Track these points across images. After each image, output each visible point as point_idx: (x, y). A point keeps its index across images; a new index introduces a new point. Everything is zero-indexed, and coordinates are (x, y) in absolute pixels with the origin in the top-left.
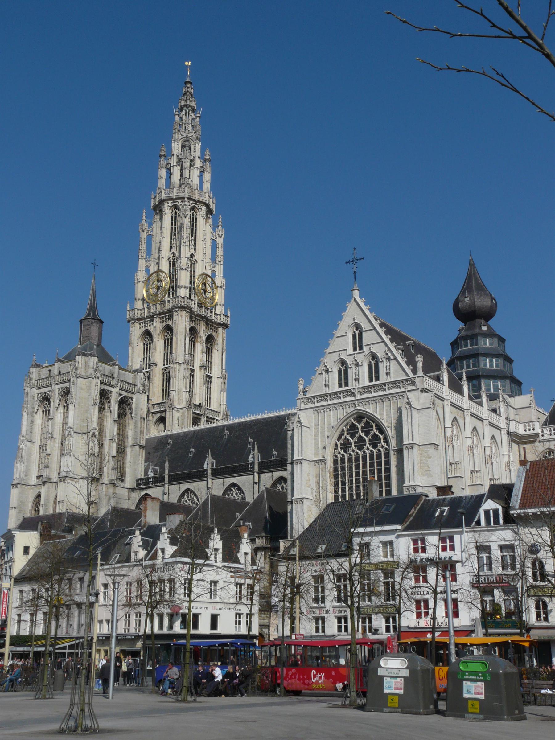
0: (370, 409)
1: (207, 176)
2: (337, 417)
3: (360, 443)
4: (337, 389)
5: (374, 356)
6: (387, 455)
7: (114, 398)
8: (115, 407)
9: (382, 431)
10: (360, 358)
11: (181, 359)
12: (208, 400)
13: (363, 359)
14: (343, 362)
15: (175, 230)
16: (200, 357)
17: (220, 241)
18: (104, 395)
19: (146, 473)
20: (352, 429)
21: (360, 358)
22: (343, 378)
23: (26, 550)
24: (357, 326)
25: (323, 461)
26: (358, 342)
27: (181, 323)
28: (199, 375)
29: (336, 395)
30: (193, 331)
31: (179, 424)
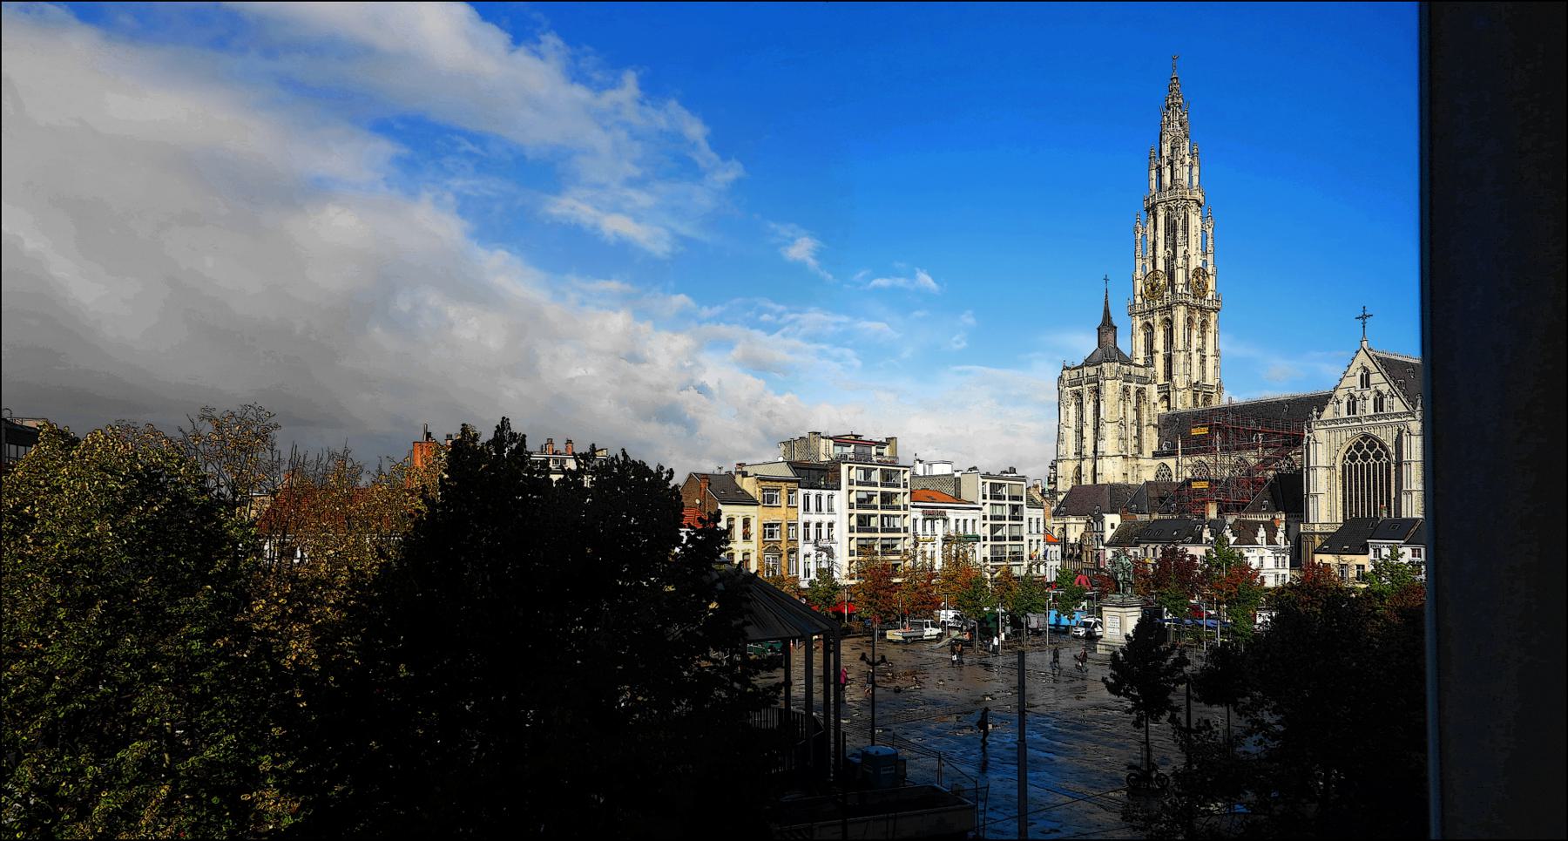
0: (1375, 433)
1: (1196, 170)
2: (1346, 438)
3: (1365, 457)
4: (1345, 415)
5: (1379, 393)
6: (1388, 464)
7: (1133, 391)
8: (1133, 398)
9: (1382, 446)
10: (1367, 393)
11: (1180, 347)
12: (1204, 379)
13: (1370, 394)
14: (1352, 396)
15: (1171, 229)
16: (1196, 342)
17: (1210, 231)
18: (1126, 390)
19: (1160, 446)
20: (1359, 447)
21: (1367, 393)
22: (1352, 407)
23: (1112, 526)
24: (1365, 369)
25: (1334, 467)
26: (1365, 381)
27: (1180, 315)
28: (1196, 357)
29: (1345, 420)
30: (1190, 321)
31: (1183, 402)
